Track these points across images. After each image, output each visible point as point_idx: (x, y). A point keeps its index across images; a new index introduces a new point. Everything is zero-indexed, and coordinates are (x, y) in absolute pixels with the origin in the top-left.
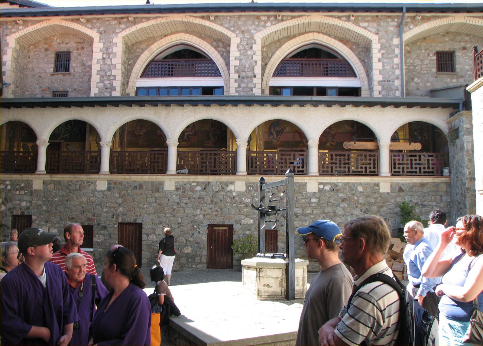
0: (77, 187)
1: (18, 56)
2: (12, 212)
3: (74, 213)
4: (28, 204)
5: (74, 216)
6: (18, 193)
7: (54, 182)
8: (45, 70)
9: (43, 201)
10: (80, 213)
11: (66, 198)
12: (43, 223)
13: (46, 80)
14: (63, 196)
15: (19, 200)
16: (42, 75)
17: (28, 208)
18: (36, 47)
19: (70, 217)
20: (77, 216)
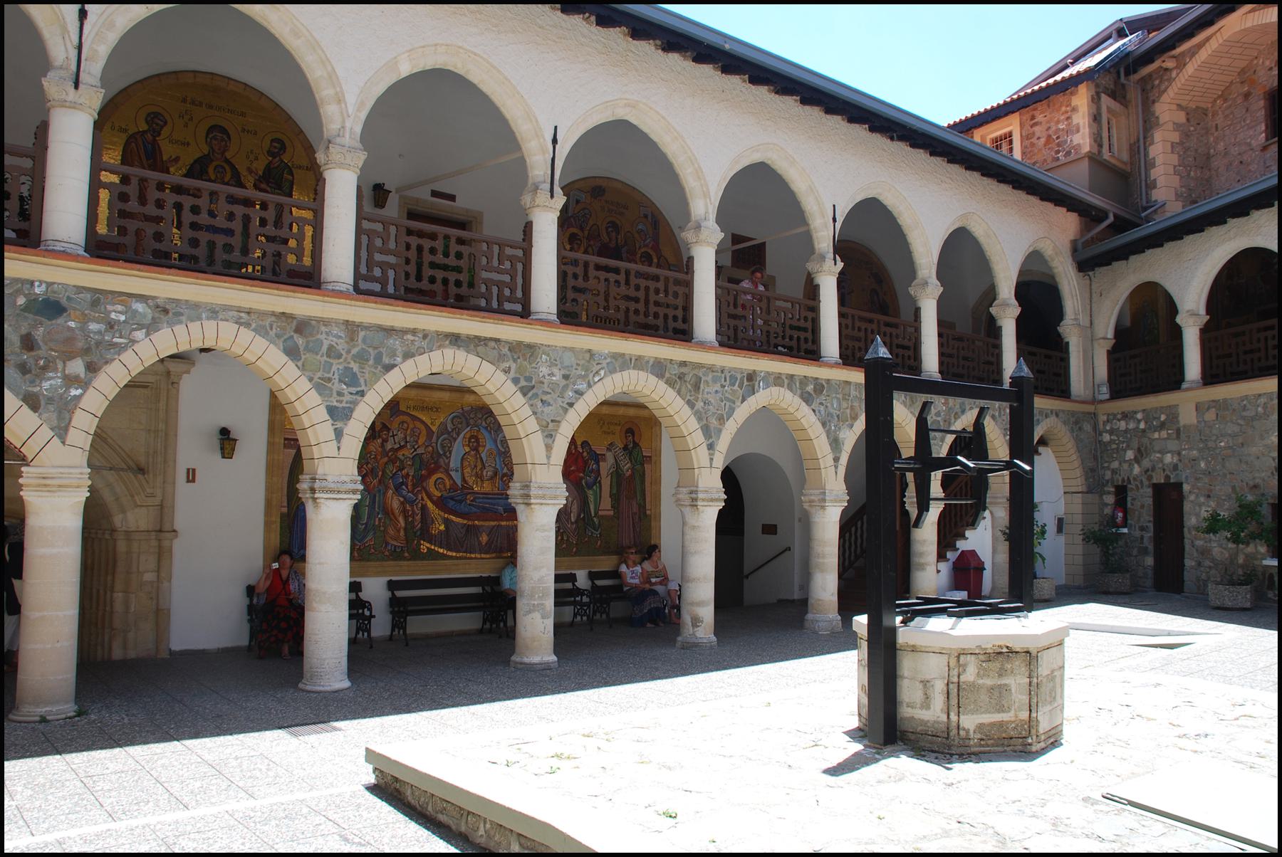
0: (1260, 409)
1: (1186, 135)
2: (1150, 478)
3: (1257, 475)
4: (1175, 459)
5: (1257, 481)
6: (1156, 435)
7: (1215, 403)
8: (1249, 144)
9: (1200, 450)
10: (1269, 474)
11: (1240, 440)
12: (1202, 499)
13: (1253, 167)
14: (1234, 436)
15: (1159, 452)
16: (1245, 158)
17: (1175, 467)
18: (1225, 100)
19: (1251, 483)
20: (1264, 480)
